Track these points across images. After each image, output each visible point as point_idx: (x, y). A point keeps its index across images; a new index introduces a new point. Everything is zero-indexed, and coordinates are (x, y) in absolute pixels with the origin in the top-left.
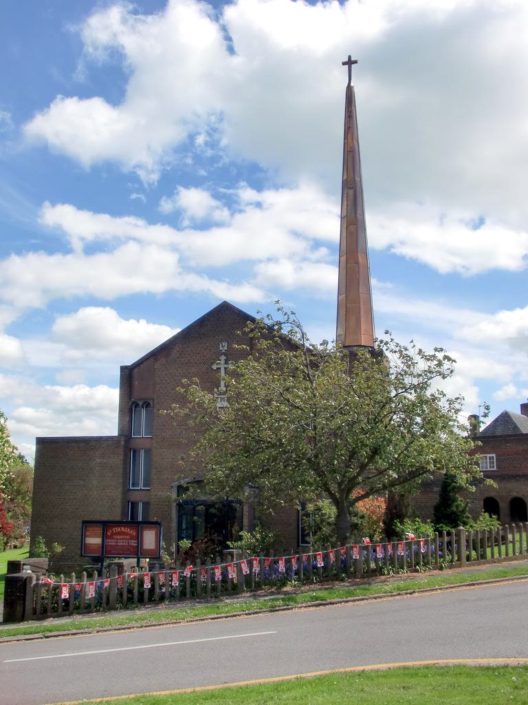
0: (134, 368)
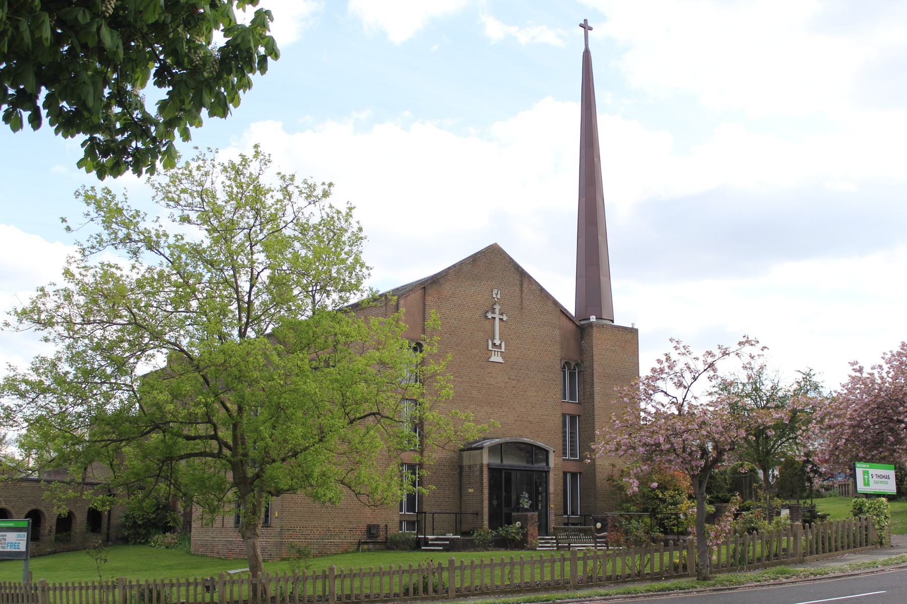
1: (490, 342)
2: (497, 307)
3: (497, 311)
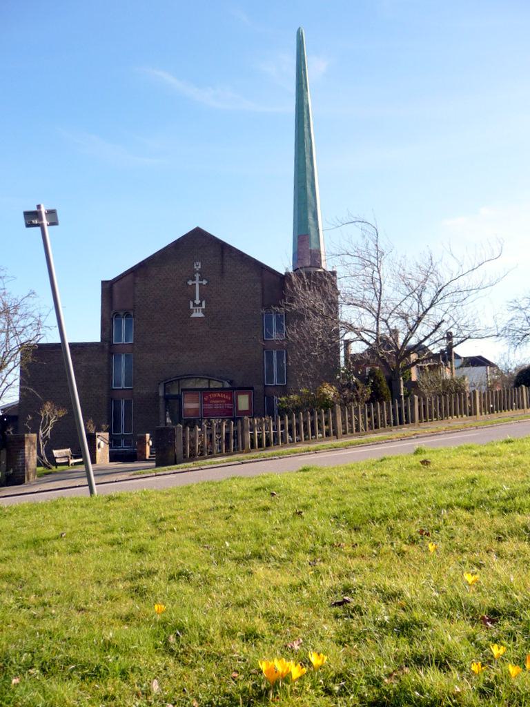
0: (114, 283)
1: (191, 303)
2: (197, 276)
3: (197, 278)
